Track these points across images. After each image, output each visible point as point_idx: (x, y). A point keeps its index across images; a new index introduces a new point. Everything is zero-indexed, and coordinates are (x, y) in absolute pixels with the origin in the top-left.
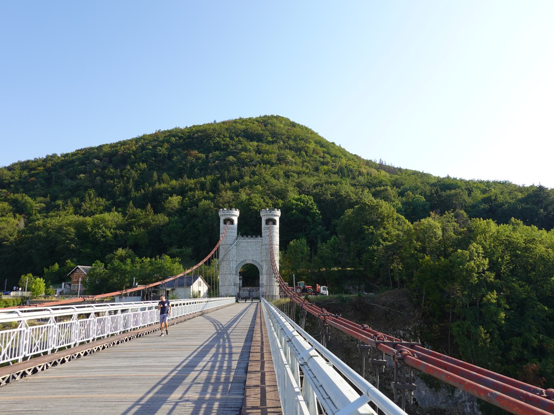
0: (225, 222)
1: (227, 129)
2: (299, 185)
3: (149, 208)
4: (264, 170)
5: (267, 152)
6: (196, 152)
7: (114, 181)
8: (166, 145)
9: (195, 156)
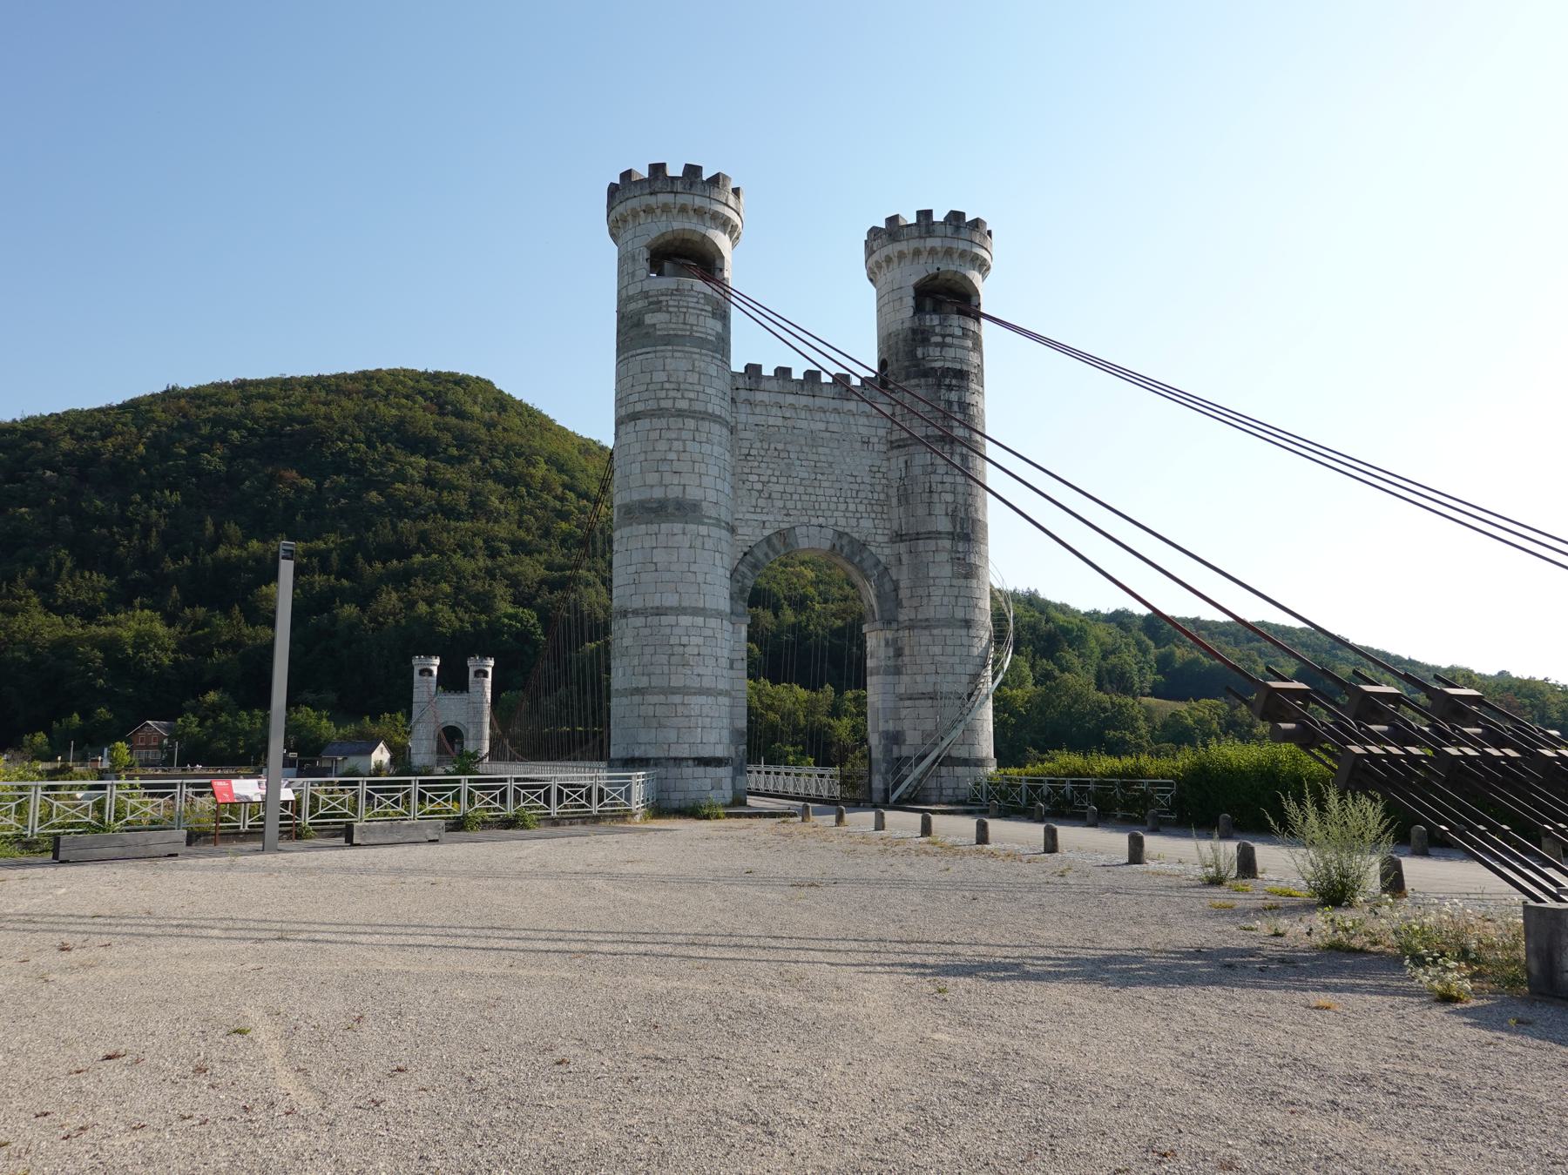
0: (422, 672)
1: (357, 418)
2: (514, 581)
3: (237, 612)
4: (445, 535)
5: (451, 487)
6: (294, 473)
7: (110, 531)
8: (219, 449)
9: (293, 485)
